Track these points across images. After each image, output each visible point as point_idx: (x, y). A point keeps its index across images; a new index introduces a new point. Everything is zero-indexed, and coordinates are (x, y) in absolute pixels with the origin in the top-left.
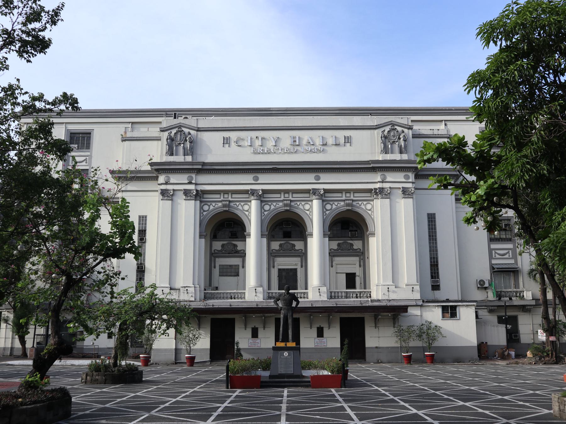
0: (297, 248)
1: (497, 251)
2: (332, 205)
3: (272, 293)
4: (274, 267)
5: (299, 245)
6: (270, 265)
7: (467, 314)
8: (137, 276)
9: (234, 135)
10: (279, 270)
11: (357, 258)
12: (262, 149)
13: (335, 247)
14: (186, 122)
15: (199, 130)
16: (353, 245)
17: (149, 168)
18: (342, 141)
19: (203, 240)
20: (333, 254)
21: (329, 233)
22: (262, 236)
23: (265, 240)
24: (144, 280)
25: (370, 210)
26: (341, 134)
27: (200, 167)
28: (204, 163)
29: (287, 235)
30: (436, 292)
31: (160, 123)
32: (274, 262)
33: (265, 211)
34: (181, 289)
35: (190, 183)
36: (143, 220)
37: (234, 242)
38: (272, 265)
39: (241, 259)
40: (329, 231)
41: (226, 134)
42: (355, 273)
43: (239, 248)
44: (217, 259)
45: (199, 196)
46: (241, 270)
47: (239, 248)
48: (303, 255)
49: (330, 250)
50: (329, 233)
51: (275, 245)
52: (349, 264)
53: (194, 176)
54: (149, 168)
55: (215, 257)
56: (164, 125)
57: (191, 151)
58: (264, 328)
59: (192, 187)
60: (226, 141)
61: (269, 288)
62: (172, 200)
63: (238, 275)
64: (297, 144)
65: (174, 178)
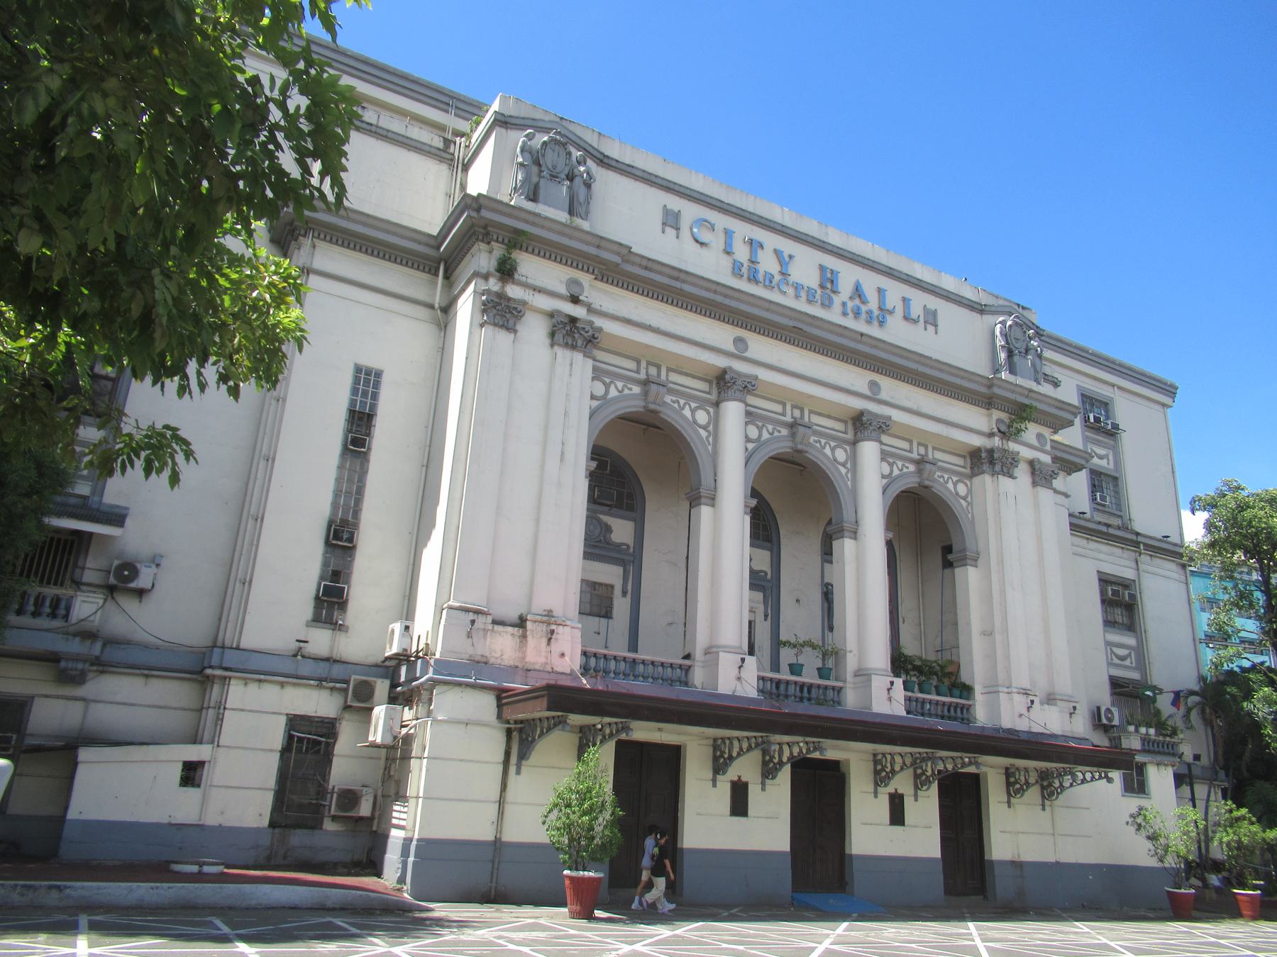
1: (1115, 650)
8: (325, 564)
9: (690, 211)
24: (347, 582)
25: (964, 498)
26: (920, 301)
27: (617, 259)
35: (575, 300)
36: (367, 382)
37: (604, 518)
41: (675, 203)
53: (585, 279)
59: (578, 312)
60: (671, 220)
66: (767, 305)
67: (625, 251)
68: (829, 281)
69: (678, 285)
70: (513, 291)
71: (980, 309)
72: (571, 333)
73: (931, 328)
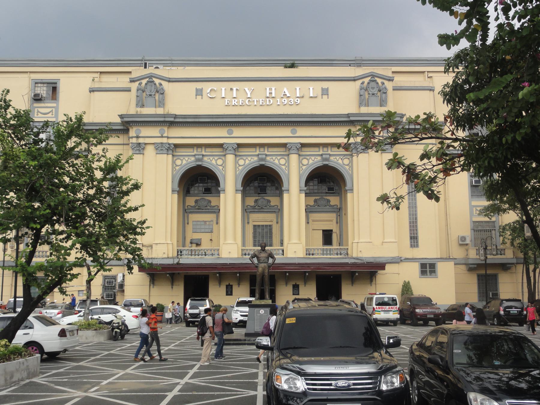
0: (272, 204)
4: (248, 223)
5: (274, 201)
6: (245, 221)
7: (447, 272)
10: (255, 226)
11: (334, 215)
12: (236, 101)
13: (312, 203)
14: (157, 72)
15: (170, 81)
17: (119, 120)
19: (176, 196)
20: (309, 210)
21: (306, 188)
23: (239, 196)
28: (176, 115)
29: (262, 191)
30: (415, 249)
31: (130, 73)
32: (248, 218)
33: (240, 166)
34: (154, 246)
35: (162, 137)
38: (246, 222)
40: (306, 186)
41: (199, 85)
42: (332, 231)
43: (213, 204)
46: (215, 226)
47: (213, 204)
48: (279, 211)
49: (307, 206)
50: (306, 188)
51: (250, 201)
52: (327, 220)
53: (166, 129)
54: (119, 120)
56: (133, 76)
57: (162, 103)
58: (239, 285)
59: (165, 140)
60: (199, 92)
61: (244, 244)
62: (143, 154)
63: (212, 232)
64: (273, 95)
65: (146, 131)
70: (141, 141)
71: (354, 79)
72: (160, 148)
73: (325, 97)
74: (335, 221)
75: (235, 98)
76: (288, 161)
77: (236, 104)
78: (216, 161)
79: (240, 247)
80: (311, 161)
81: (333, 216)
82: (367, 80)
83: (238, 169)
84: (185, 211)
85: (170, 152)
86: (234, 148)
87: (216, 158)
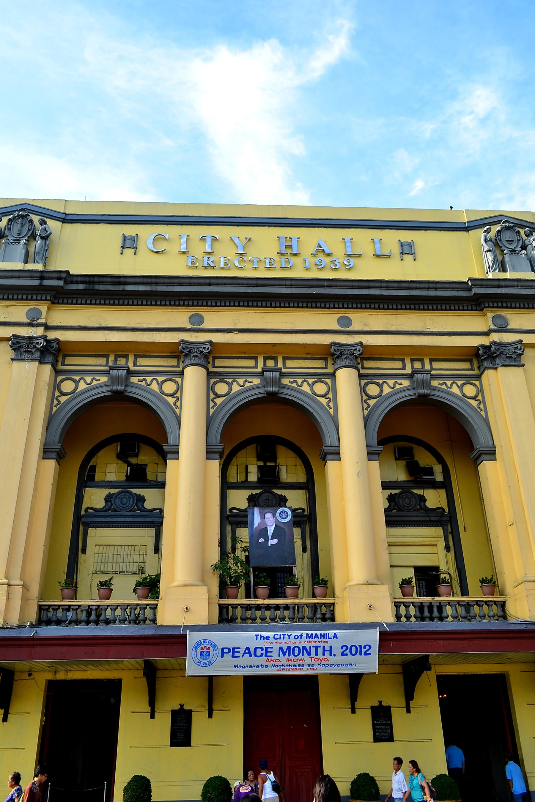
2: (381, 386)
3: (234, 607)
11: (438, 531)
16: (425, 500)
18: (396, 250)
22: (210, 453)
23: (215, 465)
26: (391, 239)
27: (61, 283)
33: (218, 396)
39: (152, 531)
41: (130, 230)
43: (148, 505)
44: (91, 531)
45: (51, 353)
47: (148, 505)
53: (43, 307)
55: (89, 525)
60: (129, 243)
66: (208, 281)
67: (64, 275)
68: (288, 250)
69: (121, 288)
71: (466, 228)
73: (408, 258)
74: (442, 544)
75: (209, 253)
76: (333, 388)
77: (212, 265)
78: (160, 385)
79: (216, 600)
80: (387, 390)
81: (434, 534)
82: (497, 228)
83: (212, 404)
84: (78, 518)
85: (50, 359)
86: (205, 351)
87: (160, 379)
